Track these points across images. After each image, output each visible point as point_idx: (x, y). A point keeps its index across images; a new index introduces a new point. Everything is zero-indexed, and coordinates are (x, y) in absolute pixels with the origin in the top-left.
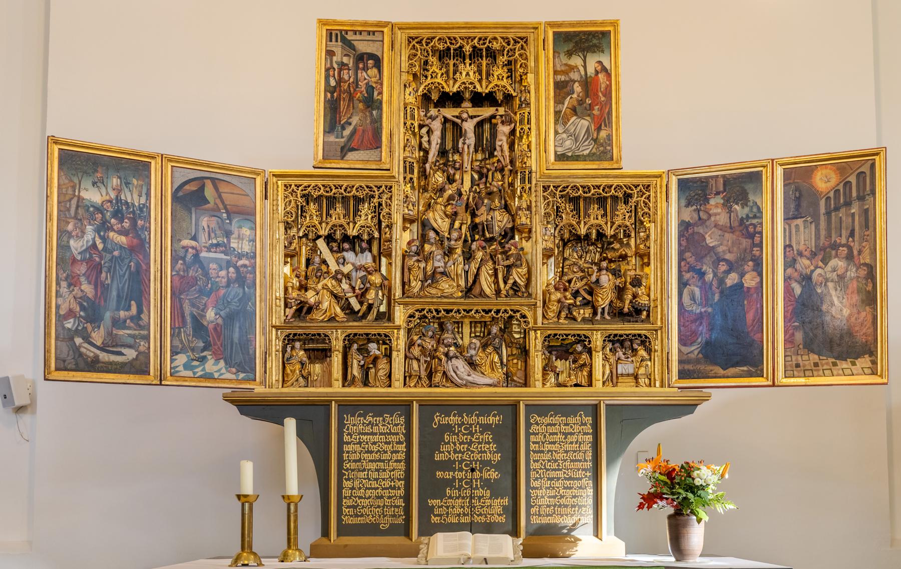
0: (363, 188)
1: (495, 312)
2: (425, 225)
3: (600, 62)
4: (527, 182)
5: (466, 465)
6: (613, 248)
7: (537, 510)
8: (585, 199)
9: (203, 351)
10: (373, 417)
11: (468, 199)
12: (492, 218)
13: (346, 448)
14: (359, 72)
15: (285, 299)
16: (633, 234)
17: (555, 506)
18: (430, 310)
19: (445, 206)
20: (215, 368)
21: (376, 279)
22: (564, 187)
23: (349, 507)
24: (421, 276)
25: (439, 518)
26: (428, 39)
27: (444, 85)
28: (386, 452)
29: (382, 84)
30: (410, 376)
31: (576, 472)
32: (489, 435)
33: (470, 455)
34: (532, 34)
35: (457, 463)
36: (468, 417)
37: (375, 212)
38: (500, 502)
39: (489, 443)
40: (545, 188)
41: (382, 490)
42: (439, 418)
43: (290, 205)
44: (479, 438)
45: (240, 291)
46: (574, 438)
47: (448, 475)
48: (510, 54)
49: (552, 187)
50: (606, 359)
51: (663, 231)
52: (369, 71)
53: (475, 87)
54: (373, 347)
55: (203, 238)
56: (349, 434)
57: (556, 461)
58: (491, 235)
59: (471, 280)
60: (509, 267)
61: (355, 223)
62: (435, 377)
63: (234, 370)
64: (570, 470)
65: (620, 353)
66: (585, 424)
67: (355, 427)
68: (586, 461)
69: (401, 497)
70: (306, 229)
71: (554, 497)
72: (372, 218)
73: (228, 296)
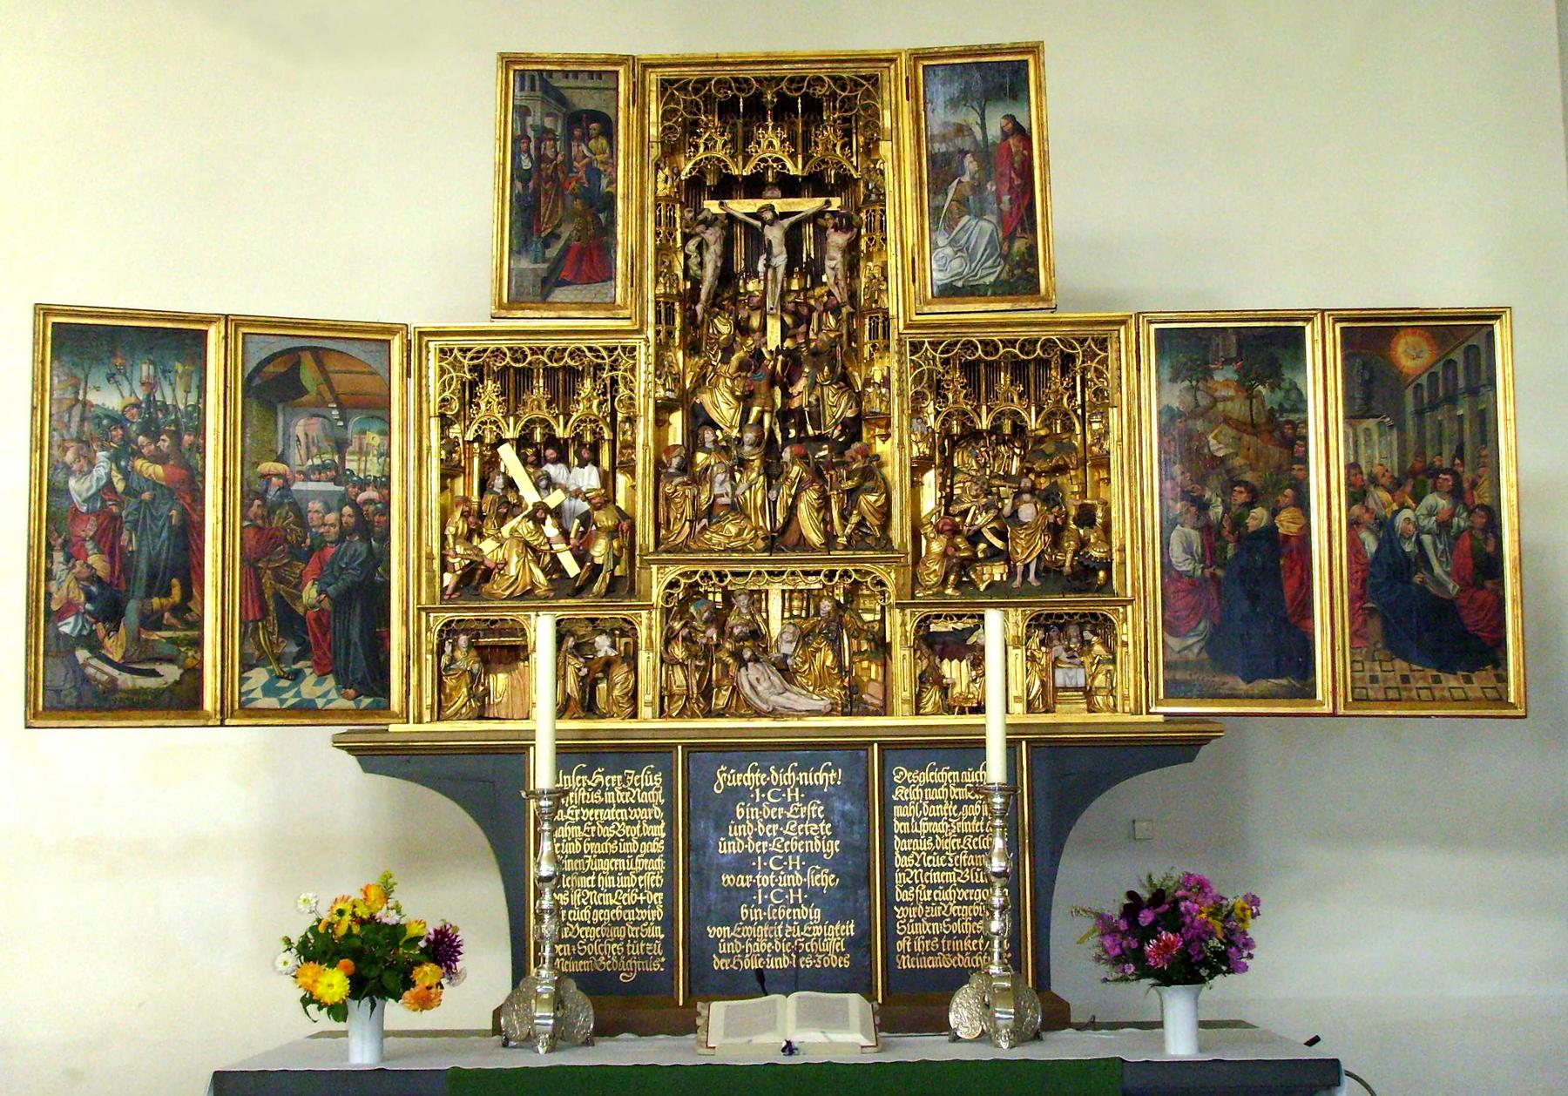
0: (583, 352)
1: (825, 576)
2: (699, 420)
3: (1012, 118)
4: (881, 337)
5: (778, 863)
6: (1043, 451)
7: (909, 944)
8: (988, 364)
9: (295, 660)
10: (604, 774)
11: (774, 367)
12: (817, 400)
14: (574, 144)
15: (443, 558)
16: (1078, 429)
18: (706, 573)
19: (732, 380)
20: (319, 690)
21: (604, 519)
22: (949, 344)
24: (688, 512)
25: (727, 961)
26: (697, 82)
27: (728, 161)
28: (629, 839)
29: (615, 166)
30: (671, 696)
31: (979, 873)
32: (819, 805)
33: (783, 844)
34: (887, 70)
35: (759, 858)
36: (778, 774)
37: (604, 394)
38: (839, 931)
39: (817, 821)
40: (916, 348)
41: (623, 909)
42: (725, 775)
43: (450, 385)
44: (799, 811)
45: (362, 548)
47: (744, 881)
48: (846, 106)
49: (926, 344)
50: (1032, 659)
51: (1135, 424)
52: (592, 143)
53: (784, 166)
54: (603, 642)
55: (297, 456)
57: (941, 852)
58: (817, 432)
59: (780, 518)
60: (852, 493)
61: (568, 416)
62: (717, 699)
63: (351, 692)
64: (967, 870)
65: (1059, 650)
69: (657, 923)
70: (480, 428)
71: (940, 919)
72: (600, 404)
73: (342, 558)
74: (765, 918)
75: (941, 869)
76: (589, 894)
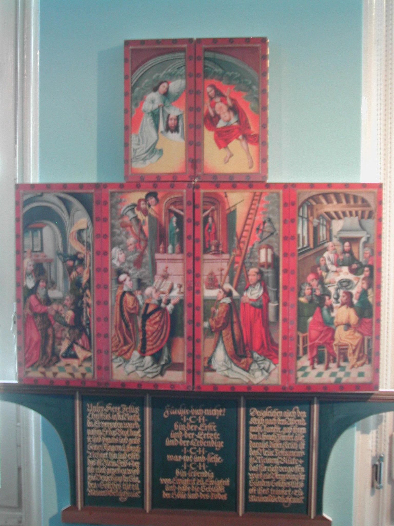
5: (193, 451)
10: (112, 406)
13: (89, 432)
17: (270, 488)
23: (93, 482)
25: (169, 494)
28: (123, 437)
39: (213, 432)
46: (289, 430)
47: (177, 458)
56: (92, 421)
57: (272, 449)
66: (299, 418)
67: (96, 415)
68: (299, 450)
69: (137, 476)
74: (187, 475)
75: (271, 457)
76: (105, 461)
